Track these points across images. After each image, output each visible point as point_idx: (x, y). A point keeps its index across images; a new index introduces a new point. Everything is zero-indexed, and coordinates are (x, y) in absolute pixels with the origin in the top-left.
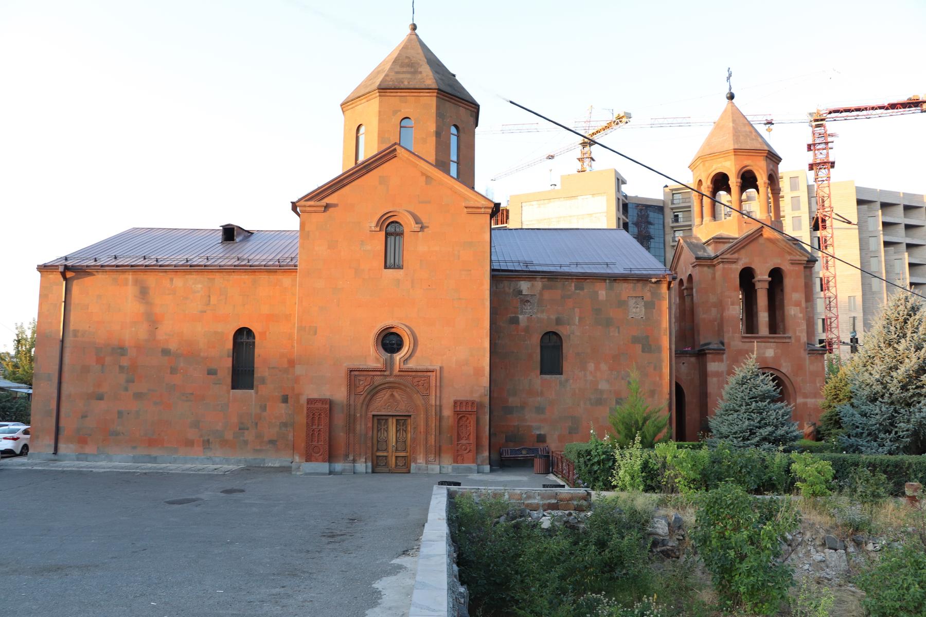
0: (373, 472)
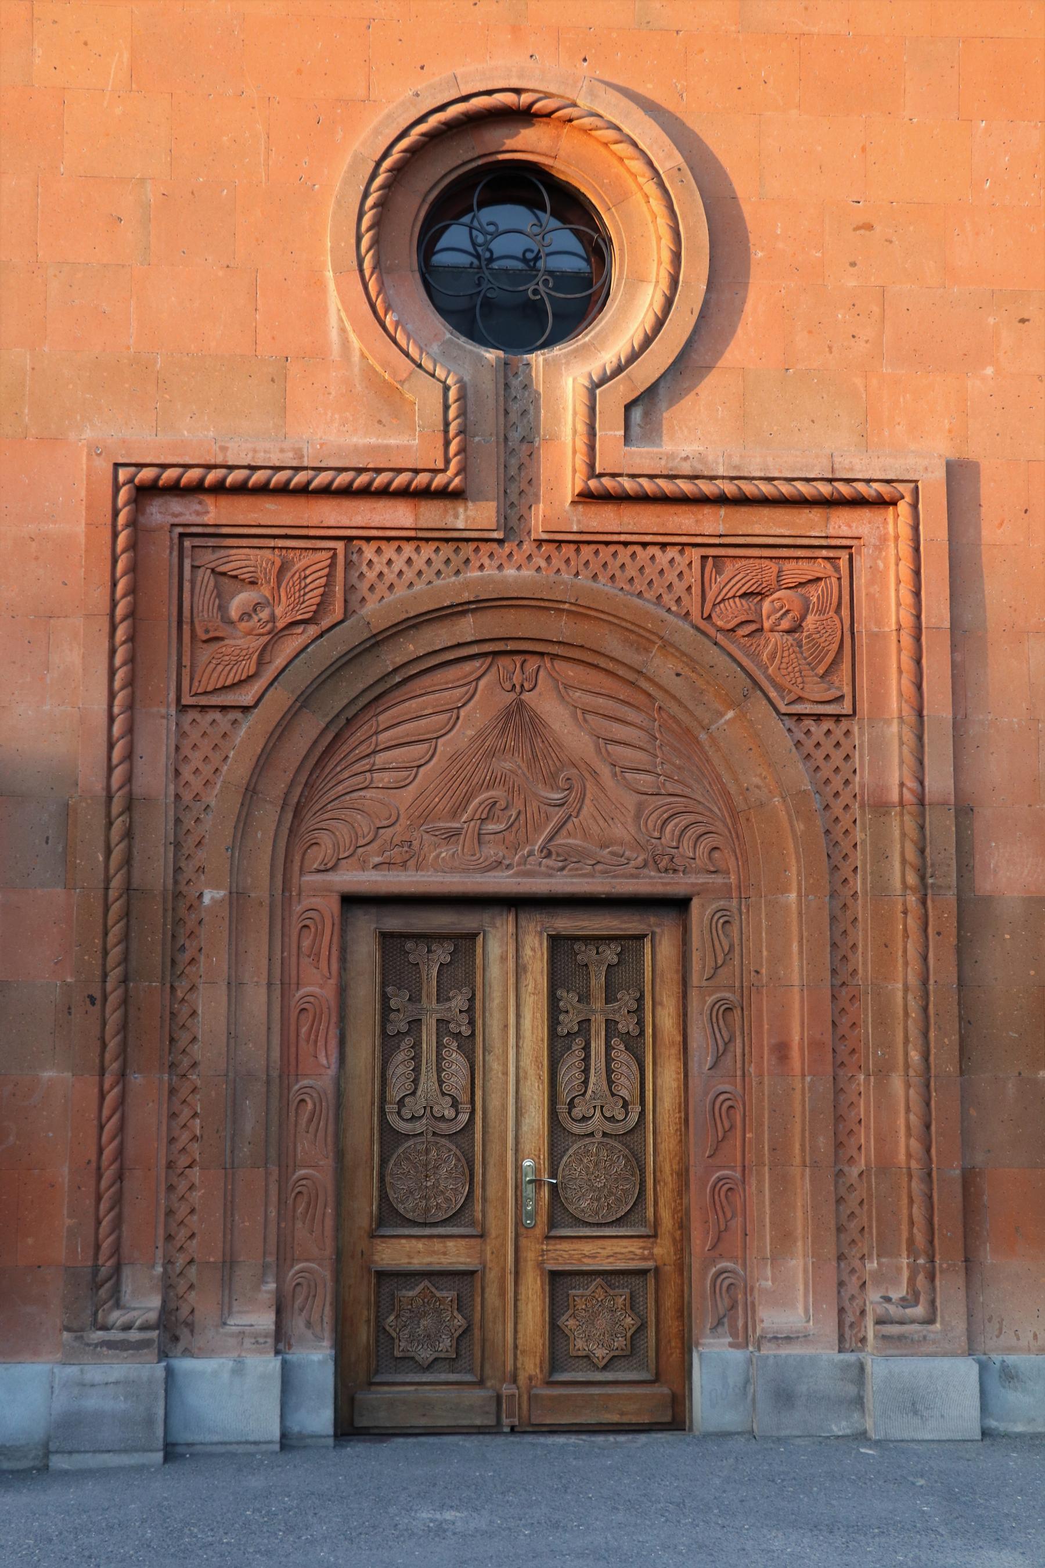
0: (349, 1428)
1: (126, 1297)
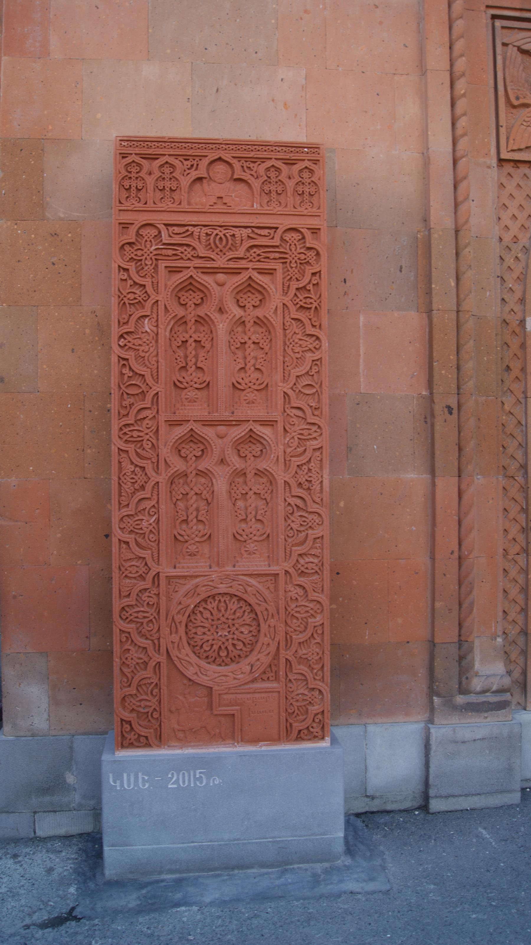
1: (477, 666)
